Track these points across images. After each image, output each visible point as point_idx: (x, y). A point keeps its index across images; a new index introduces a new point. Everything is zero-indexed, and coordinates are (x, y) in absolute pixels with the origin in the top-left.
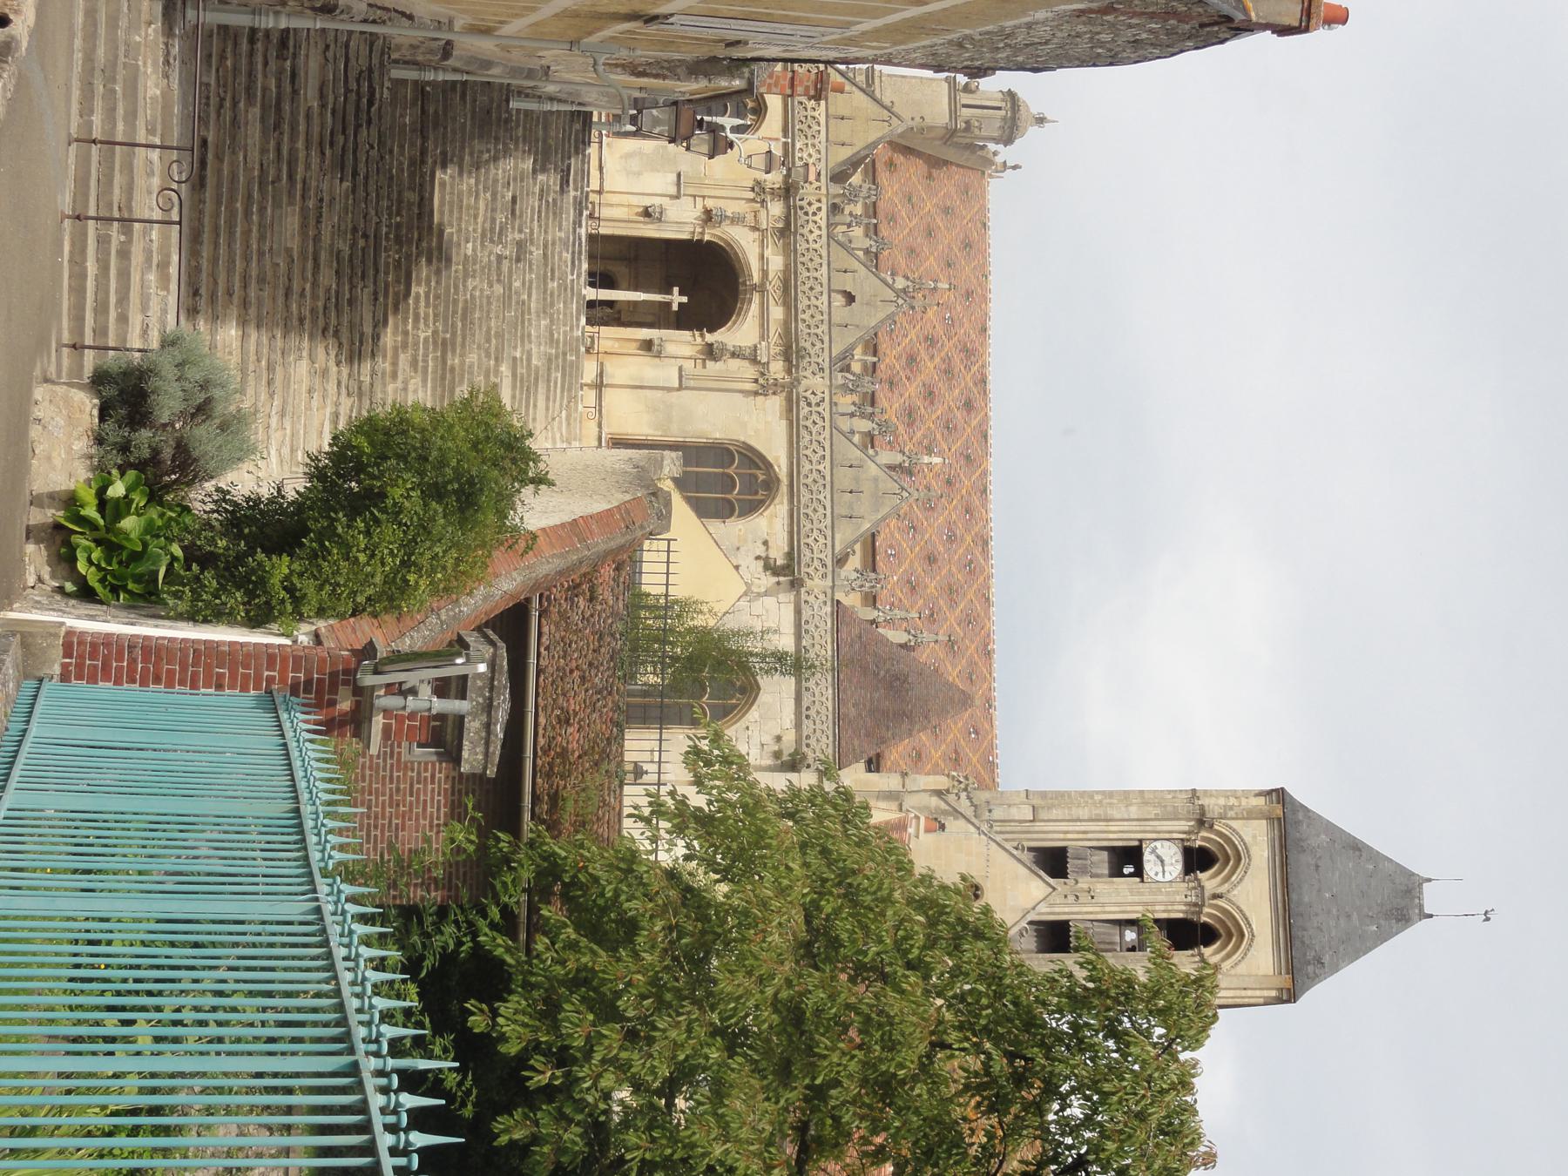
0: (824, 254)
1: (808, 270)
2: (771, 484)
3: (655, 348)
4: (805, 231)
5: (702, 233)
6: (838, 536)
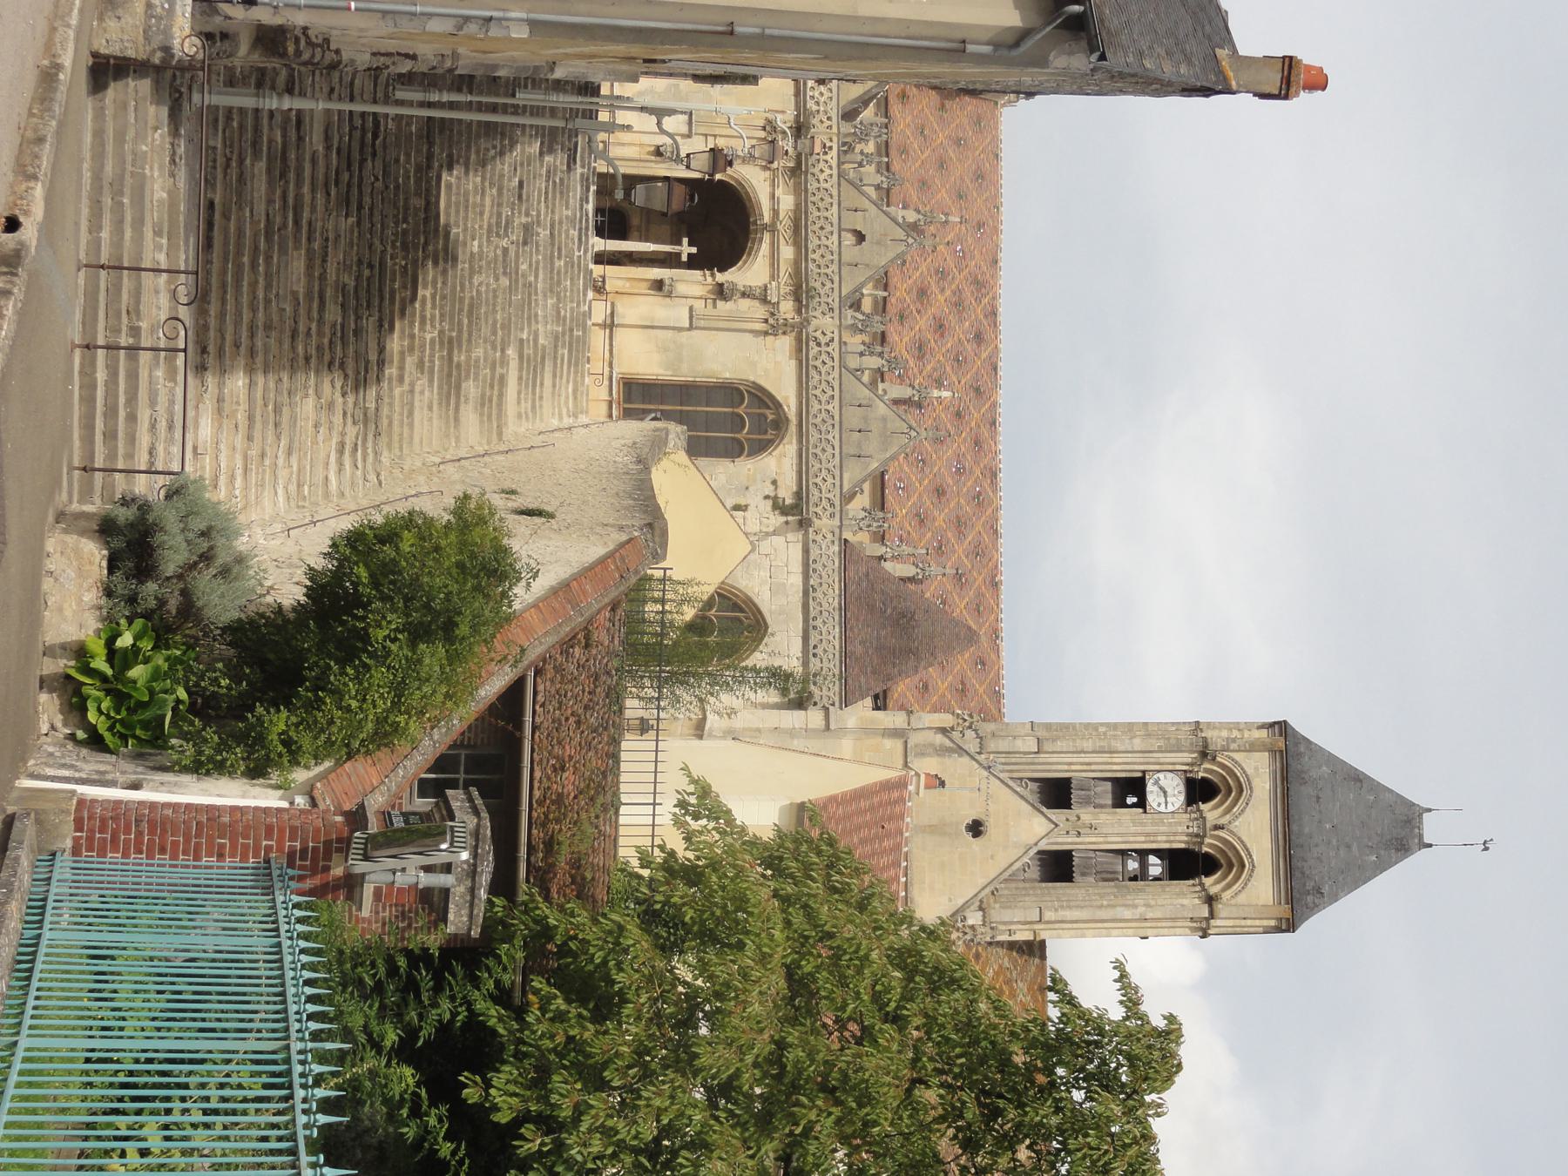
0: (835, 193)
1: (819, 209)
2: (780, 424)
3: (666, 288)
4: (816, 171)
6: (846, 476)
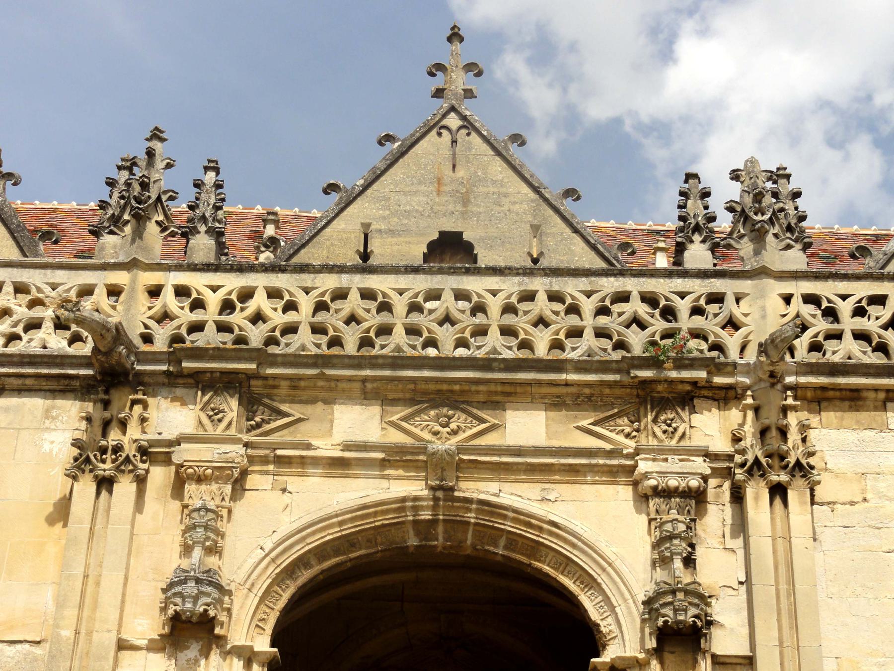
0: (329, 282)
4: (256, 335)
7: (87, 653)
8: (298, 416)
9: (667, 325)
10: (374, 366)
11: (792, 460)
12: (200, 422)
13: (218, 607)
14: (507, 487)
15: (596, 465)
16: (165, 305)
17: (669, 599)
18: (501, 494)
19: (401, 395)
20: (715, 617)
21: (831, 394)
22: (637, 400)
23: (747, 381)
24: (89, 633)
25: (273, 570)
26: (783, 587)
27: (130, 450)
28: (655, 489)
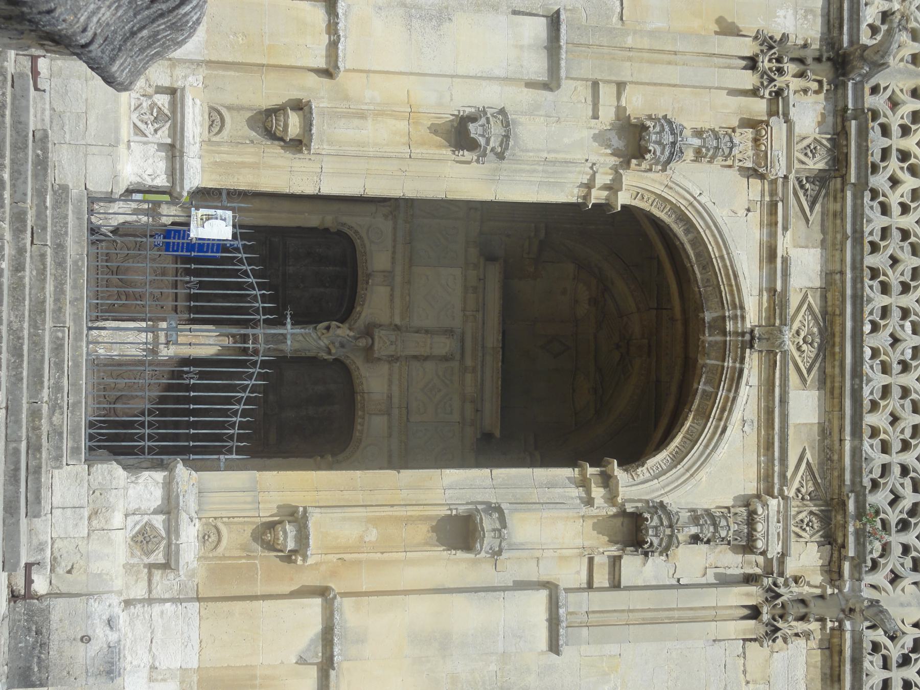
4: (879, 181)
5: (613, 187)
7: (614, 59)
8: (811, 219)
9: (893, 524)
10: (854, 281)
11: (780, 624)
12: (804, 138)
13: (653, 161)
14: (754, 391)
15: (773, 465)
16: (904, 103)
17: (665, 523)
18: (748, 387)
19: (830, 303)
20: (651, 559)
21: (836, 658)
22: (828, 499)
23: (846, 590)
24: (630, 59)
25: (683, 204)
26: (676, 614)
27: (780, 82)
28: (755, 512)
